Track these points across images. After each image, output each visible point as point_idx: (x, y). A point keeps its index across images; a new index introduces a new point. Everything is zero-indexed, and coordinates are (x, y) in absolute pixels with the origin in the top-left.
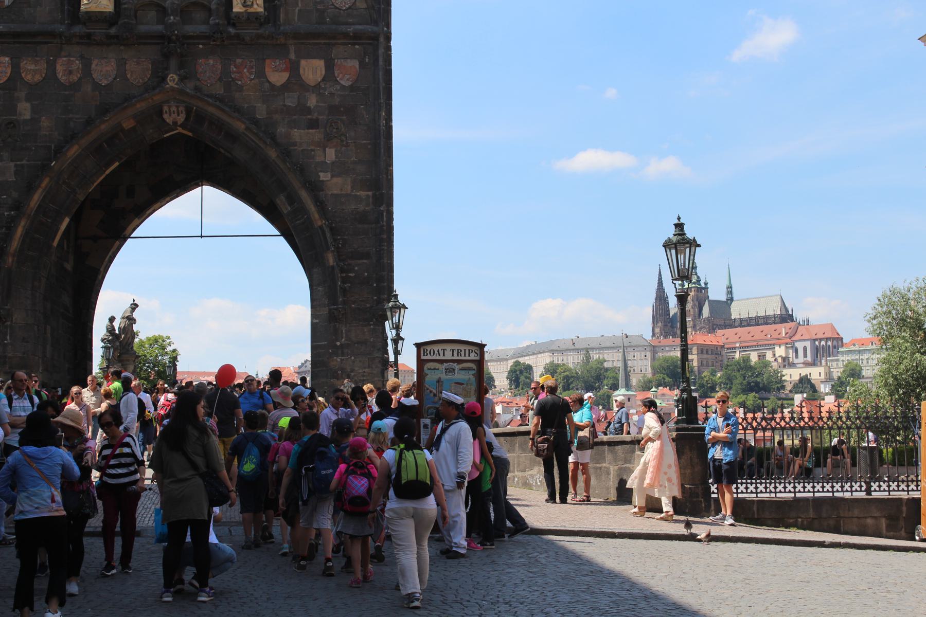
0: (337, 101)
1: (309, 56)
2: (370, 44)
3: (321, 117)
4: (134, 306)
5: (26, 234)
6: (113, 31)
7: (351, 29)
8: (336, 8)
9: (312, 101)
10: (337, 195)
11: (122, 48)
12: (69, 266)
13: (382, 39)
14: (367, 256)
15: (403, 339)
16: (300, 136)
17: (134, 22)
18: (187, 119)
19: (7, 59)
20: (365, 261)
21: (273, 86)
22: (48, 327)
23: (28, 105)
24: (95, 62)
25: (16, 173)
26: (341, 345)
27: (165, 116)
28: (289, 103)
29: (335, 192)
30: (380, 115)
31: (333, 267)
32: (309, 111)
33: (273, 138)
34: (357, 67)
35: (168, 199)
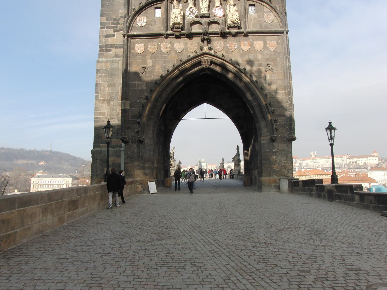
0: (268, 57)
1: (257, 40)
2: (280, 35)
3: (263, 63)
5: (150, 109)
6: (183, 32)
7: (273, 30)
11: (186, 39)
12: (163, 128)
13: (285, 32)
19: (143, 44)
20: (283, 118)
23: (151, 61)
25: (146, 86)
26: (275, 151)
27: (202, 64)
34: (276, 44)
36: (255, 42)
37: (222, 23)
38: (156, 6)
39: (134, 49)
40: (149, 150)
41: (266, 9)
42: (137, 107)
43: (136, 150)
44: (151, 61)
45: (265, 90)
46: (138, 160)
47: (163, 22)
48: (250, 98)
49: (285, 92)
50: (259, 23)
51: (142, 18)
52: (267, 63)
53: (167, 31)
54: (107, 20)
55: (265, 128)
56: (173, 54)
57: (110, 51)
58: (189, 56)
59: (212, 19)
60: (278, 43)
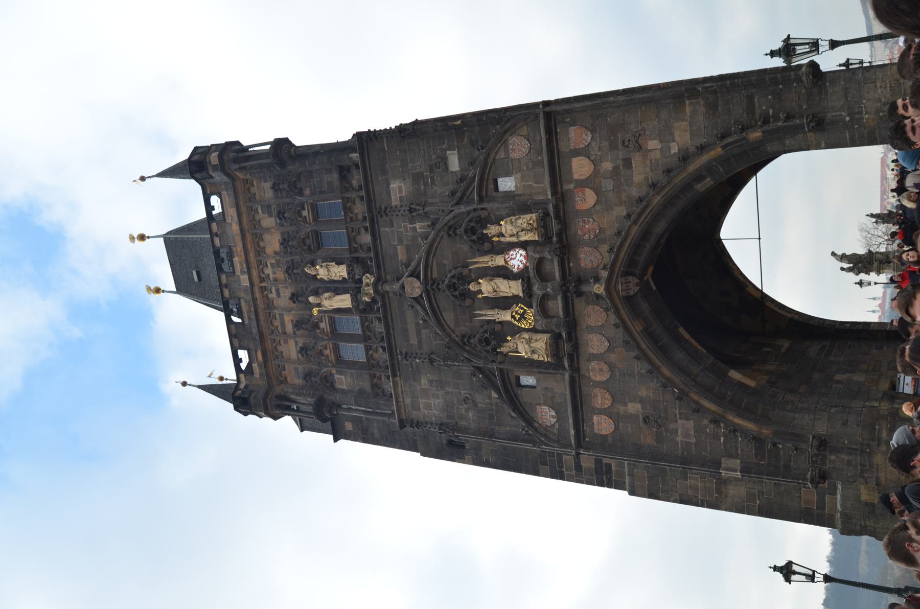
0: (605, 144)
3: (621, 157)
9: (607, 166)
10: (692, 135)
12: (786, 344)
13: (548, 109)
14: (750, 98)
15: (848, 60)
16: (640, 174)
17: (555, 320)
18: (633, 274)
20: (756, 100)
21: (597, 202)
22: (838, 377)
23: (630, 405)
24: (591, 350)
25: (687, 420)
26: (849, 115)
27: (631, 293)
28: (610, 187)
29: (689, 137)
30: (614, 102)
31: (763, 132)
32: (616, 168)
33: (641, 200)
35: (731, 264)
36: (576, 177)
37: (538, 252)
38: (514, 384)
39: (607, 436)
40: (845, 424)
41: (502, 155)
42: (737, 442)
43: (843, 456)
44: (630, 405)
46: (870, 454)
47: (546, 373)
48: (708, 182)
49: (689, 98)
50: (533, 168)
51: (540, 415)
52: (620, 147)
53: (564, 368)
54: (545, 464)
55: (784, 145)
56: (612, 357)
57: (609, 466)
58: (616, 326)
60: (573, 124)
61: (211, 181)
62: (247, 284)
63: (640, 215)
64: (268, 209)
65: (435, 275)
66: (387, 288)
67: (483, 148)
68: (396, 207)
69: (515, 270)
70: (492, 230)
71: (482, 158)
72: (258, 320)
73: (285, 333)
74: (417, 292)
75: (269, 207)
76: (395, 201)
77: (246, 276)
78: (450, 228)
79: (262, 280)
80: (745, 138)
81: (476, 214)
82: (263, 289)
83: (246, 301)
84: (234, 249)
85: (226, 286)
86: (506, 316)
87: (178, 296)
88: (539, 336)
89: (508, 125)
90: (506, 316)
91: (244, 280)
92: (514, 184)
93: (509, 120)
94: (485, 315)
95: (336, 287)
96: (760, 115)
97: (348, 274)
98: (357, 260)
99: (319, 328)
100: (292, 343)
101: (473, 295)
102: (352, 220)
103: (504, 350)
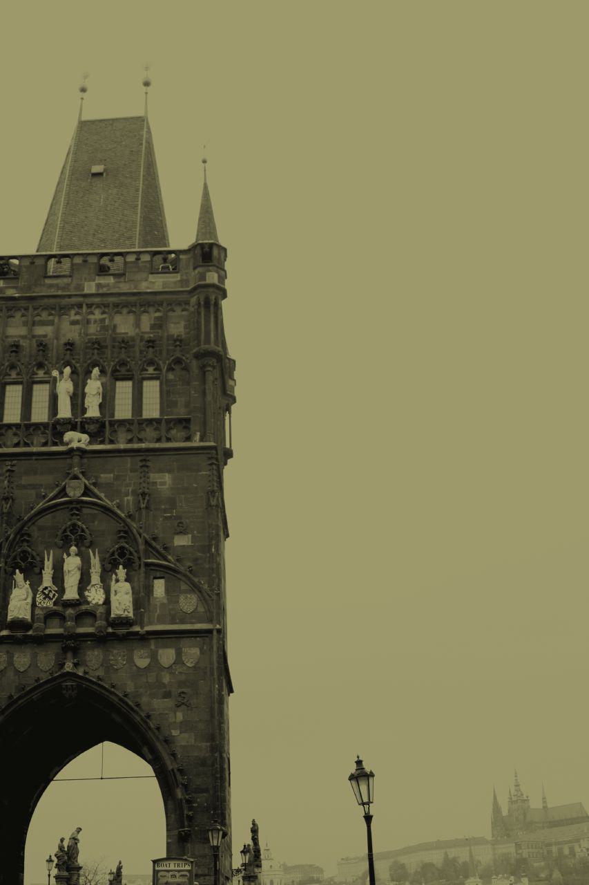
0: (183, 677)
1: (166, 647)
4: (79, 830)
6: (30, 633)
8: (184, 612)
9: (166, 679)
10: (184, 747)
11: (35, 645)
13: (215, 633)
14: (206, 790)
20: (205, 794)
24: (16, 656)
28: (150, 681)
29: (183, 744)
30: (214, 686)
31: (181, 799)
32: (164, 685)
33: (138, 705)
34: (199, 653)
36: (160, 651)
37: (101, 616)
41: (184, 587)
45: (174, 743)
49: (211, 745)
52: (180, 690)
56: (10, 674)
58: (37, 680)
59: (84, 607)
60: (202, 652)
61: (191, 267)
62: (86, 291)
63: (127, 704)
64: (159, 325)
65: (85, 511)
66: (76, 460)
67: (191, 571)
68: (148, 478)
69: (86, 593)
70: (121, 572)
71: (182, 569)
72: (48, 297)
73: (34, 324)
74: (70, 492)
75: (160, 327)
76: (154, 477)
77: (93, 291)
78: (125, 532)
79: (89, 306)
80: (178, 786)
81: (136, 559)
82: (80, 306)
83: (68, 285)
84: (122, 279)
85: (85, 261)
86: (47, 580)
87: (75, 124)
88: (29, 611)
89: (207, 597)
90: (47, 580)
91: (90, 288)
92: (158, 596)
93: (210, 597)
94: (48, 560)
95: (78, 399)
96: (194, 798)
97: (90, 418)
98: (103, 425)
99: (37, 369)
100: (23, 331)
101: (65, 547)
102: (139, 424)
103: (19, 576)
